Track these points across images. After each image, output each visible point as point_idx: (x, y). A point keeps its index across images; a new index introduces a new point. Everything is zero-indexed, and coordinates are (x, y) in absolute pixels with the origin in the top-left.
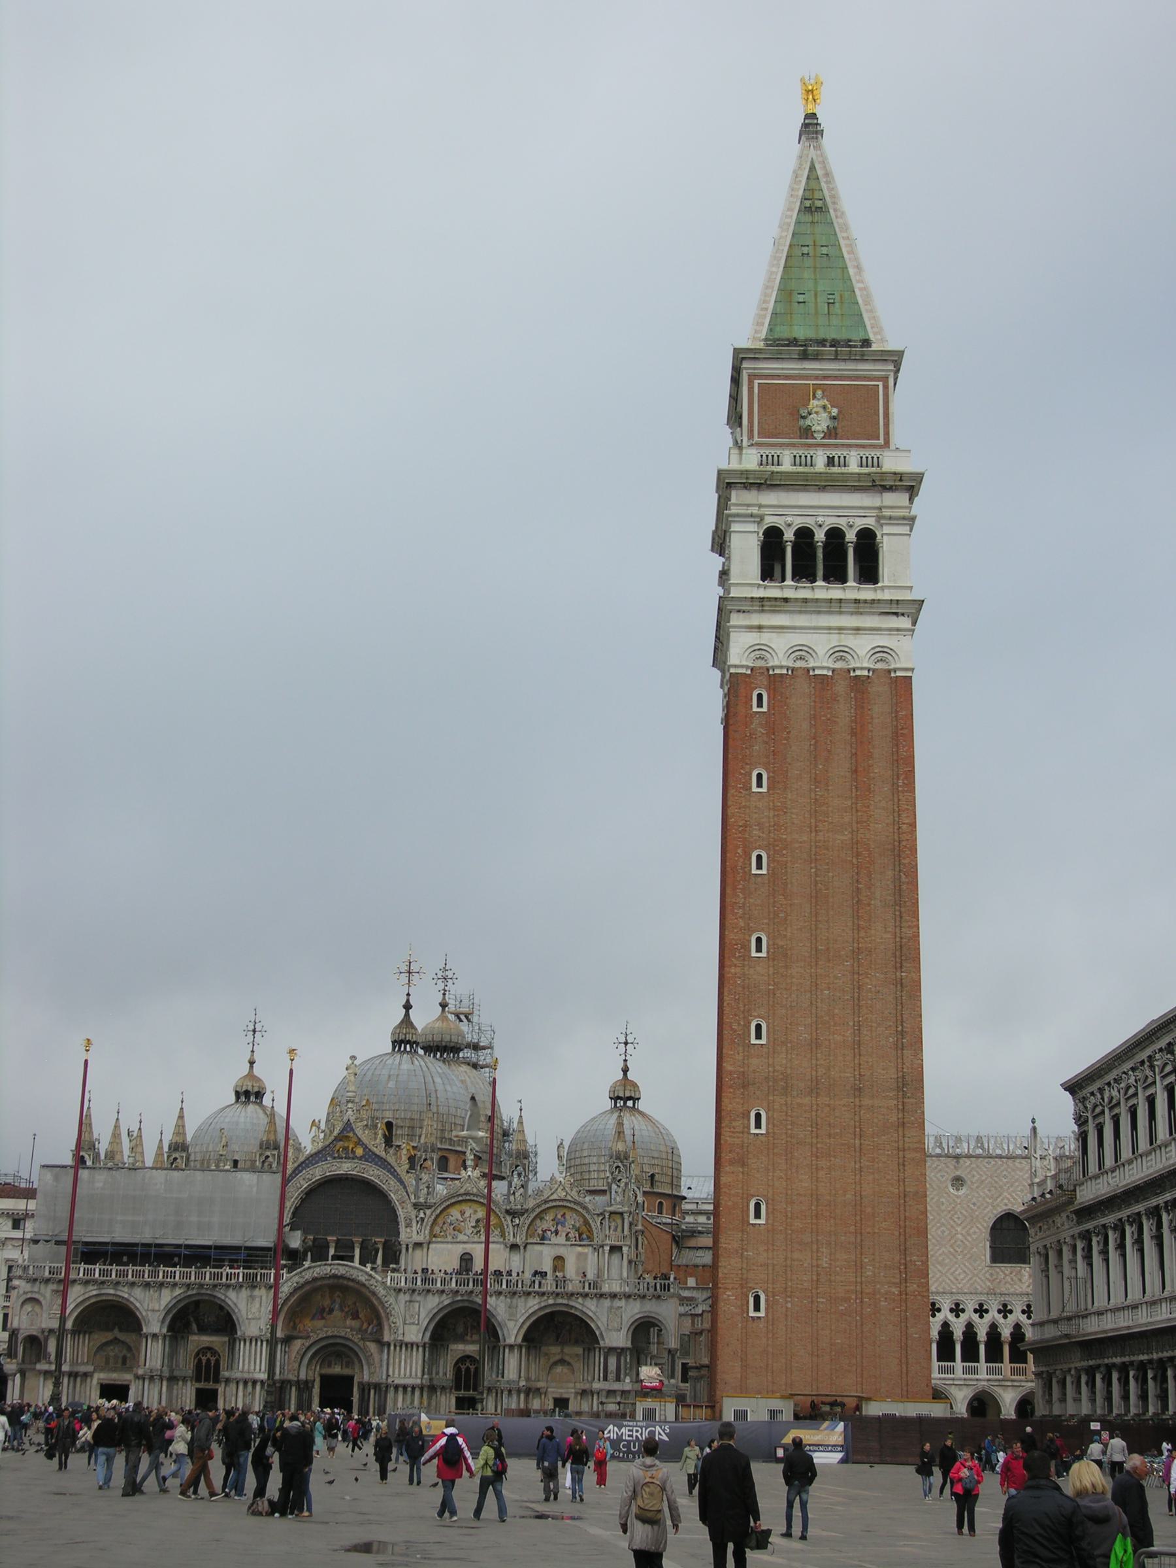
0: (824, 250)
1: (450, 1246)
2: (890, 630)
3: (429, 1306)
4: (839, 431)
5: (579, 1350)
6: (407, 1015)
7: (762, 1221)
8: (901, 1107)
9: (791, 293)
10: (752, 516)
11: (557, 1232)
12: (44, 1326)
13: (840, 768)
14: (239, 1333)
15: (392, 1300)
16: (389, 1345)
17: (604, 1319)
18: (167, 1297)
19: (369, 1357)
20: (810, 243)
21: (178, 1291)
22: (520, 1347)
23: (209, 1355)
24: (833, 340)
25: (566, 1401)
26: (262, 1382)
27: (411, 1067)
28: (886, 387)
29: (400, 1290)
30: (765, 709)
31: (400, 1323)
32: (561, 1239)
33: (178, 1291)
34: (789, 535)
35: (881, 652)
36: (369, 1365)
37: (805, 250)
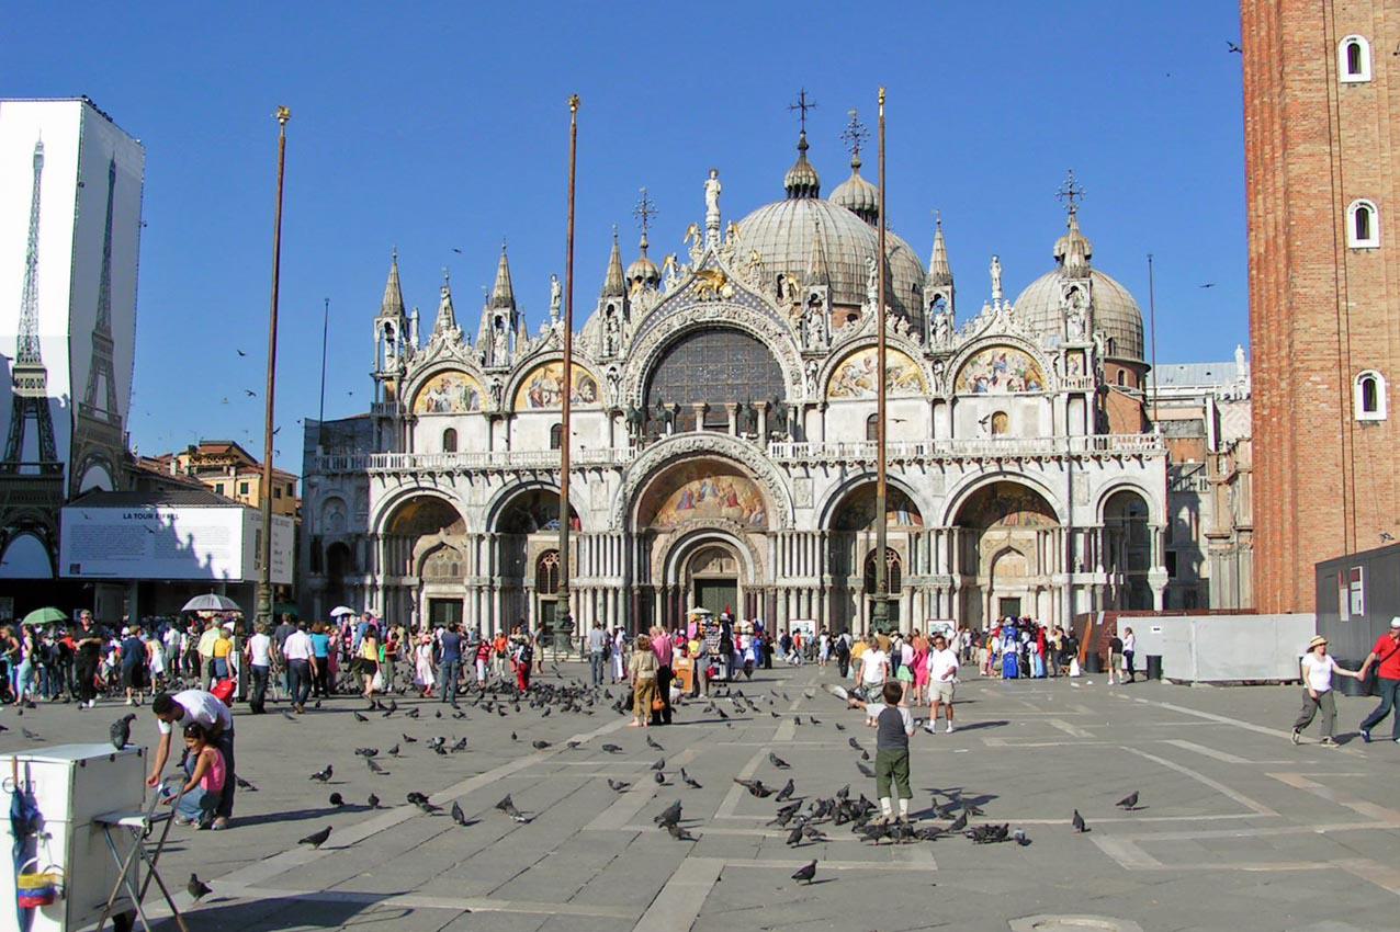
1: (852, 406)
3: (824, 485)
11: (995, 381)
12: (350, 530)
14: (584, 529)
15: (777, 478)
16: (776, 537)
18: (493, 488)
19: (754, 552)
22: (950, 531)
25: (1019, 599)
26: (616, 591)
27: (807, 211)
29: (785, 465)
32: (1001, 389)
36: (757, 561)
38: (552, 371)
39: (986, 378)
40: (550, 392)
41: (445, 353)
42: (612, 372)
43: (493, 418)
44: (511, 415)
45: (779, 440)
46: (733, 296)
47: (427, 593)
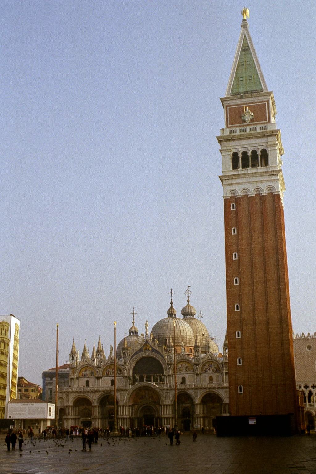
0: (249, 63)
1: (179, 375)
2: (272, 180)
3: (171, 394)
4: (254, 119)
5: (218, 404)
6: (172, 306)
7: (241, 365)
8: (281, 327)
9: (238, 78)
10: (228, 150)
13: (257, 225)
17: (224, 395)
20: (244, 61)
21: (100, 393)
22: (200, 404)
23: (112, 411)
24: (251, 91)
26: (126, 418)
28: (268, 104)
29: (164, 389)
30: (235, 209)
31: (164, 399)
32: (211, 371)
33: (100, 393)
34: (240, 154)
35: (270, 188)
37: (243, 63)
38: (111, 367)
39: (208, 369)
40: (111, 372)
41: (87, 363)
42: (125, 368)
43: (98, 378)
44: (101, 377)
45: (162, 384)
46: (152, 350)
47: (82, 420)
